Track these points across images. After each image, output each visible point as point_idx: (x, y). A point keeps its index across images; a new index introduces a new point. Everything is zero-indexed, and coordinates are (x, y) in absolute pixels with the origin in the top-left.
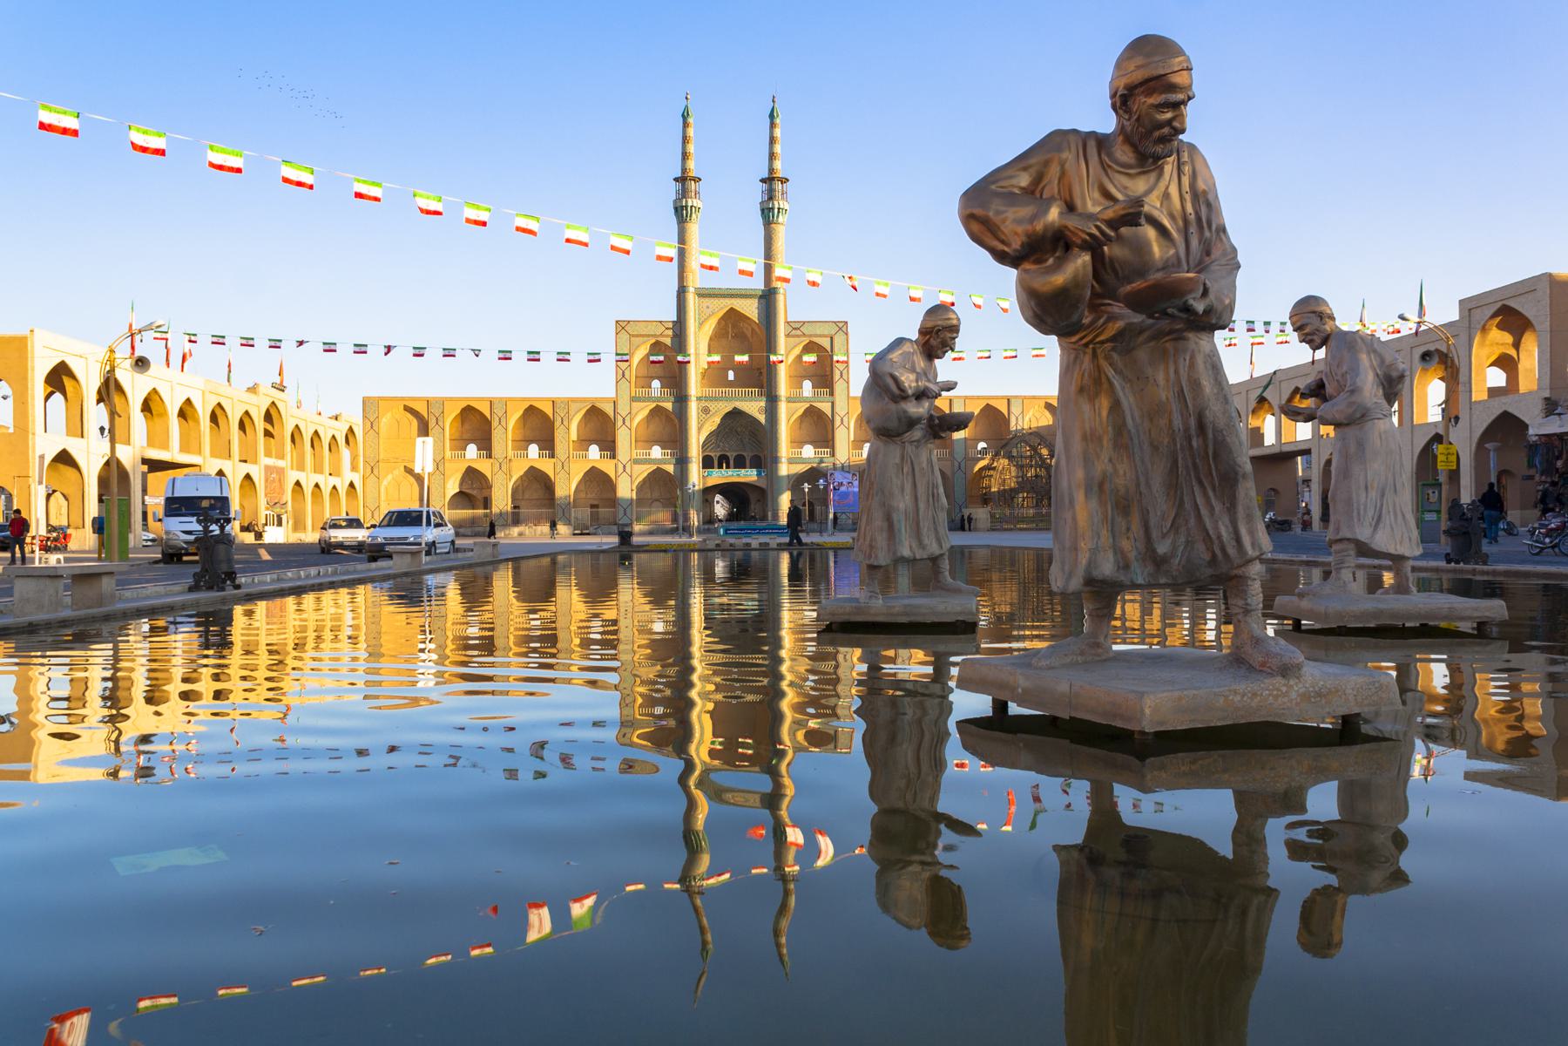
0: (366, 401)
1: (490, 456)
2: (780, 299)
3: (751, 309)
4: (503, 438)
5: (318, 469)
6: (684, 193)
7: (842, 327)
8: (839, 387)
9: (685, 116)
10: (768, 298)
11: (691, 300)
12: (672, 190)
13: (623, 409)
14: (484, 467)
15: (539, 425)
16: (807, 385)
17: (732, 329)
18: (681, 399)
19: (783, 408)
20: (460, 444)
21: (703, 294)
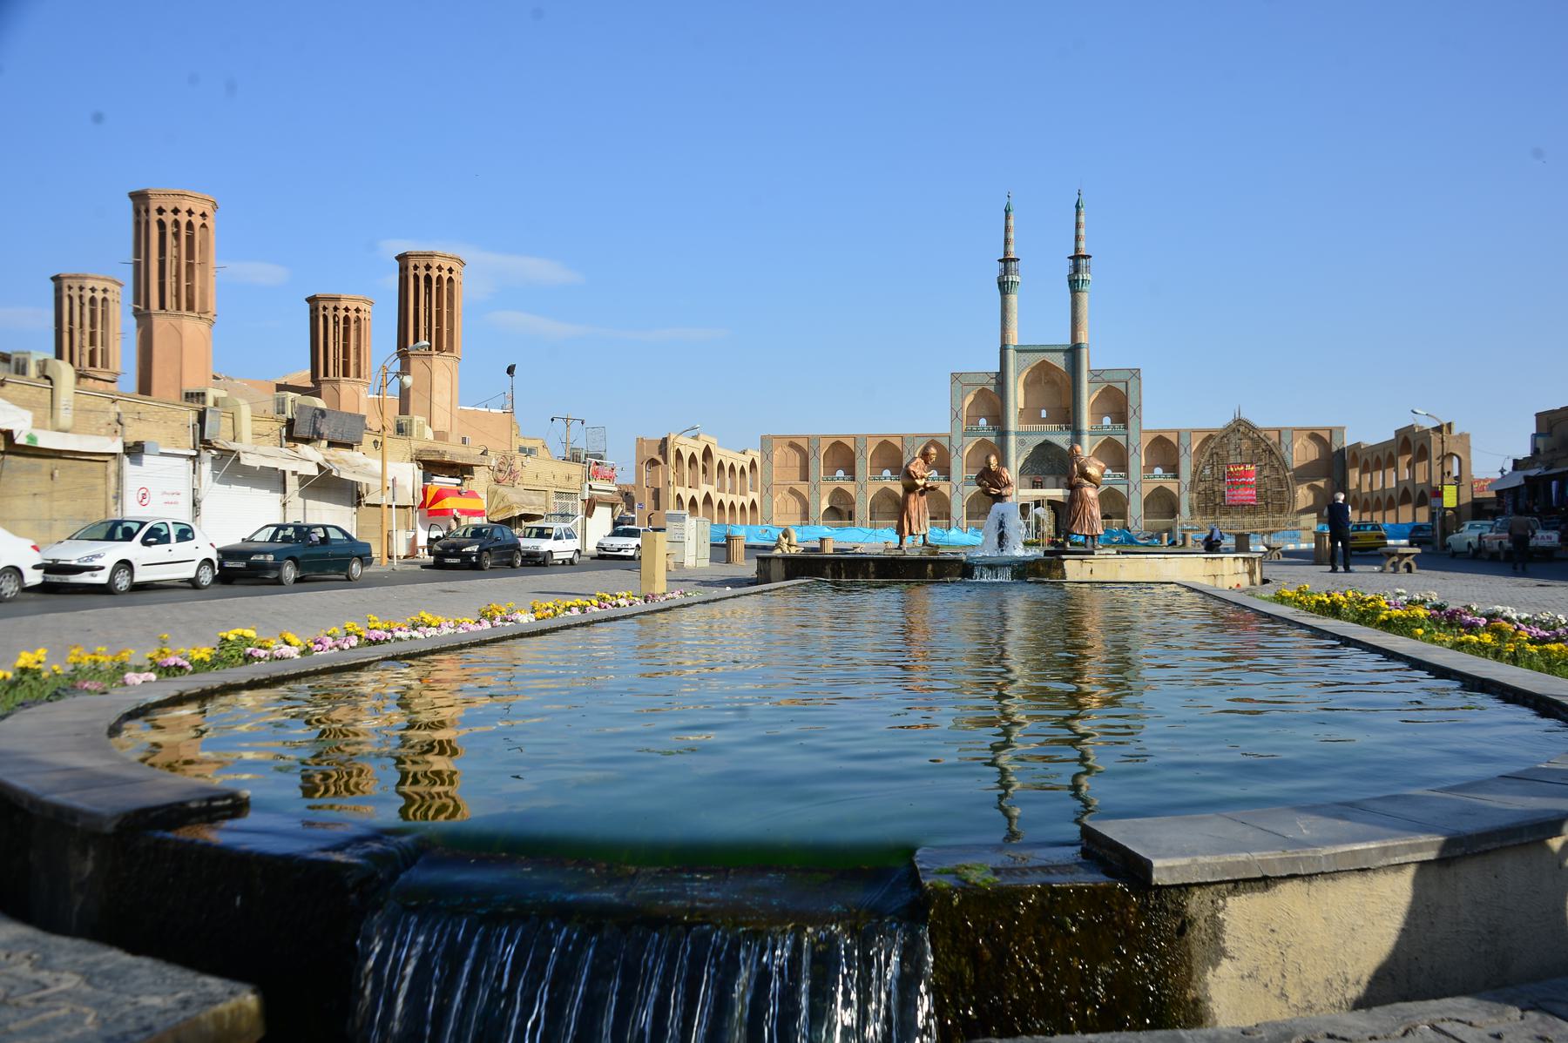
0: (763, 438)
1: (853, 479)
2: (1084, 352)
3: (1059, 361)
4: (863, 467)
5: (733, 491)
6: (1006, 271)
7: (1136, 373)
8: (1132, 423)
9: (1007, 212)
10: (1073, 352)
11: (1011, 353)
12: (997, 268)
13: (956, 443)
14: (849, 487)
15: (890, 455)
16: (1107, 421)
17: (1041, 376)
18: (1003, 434)
19: (1086, 439)
20: (830, 471)
21: (1020, 350)
